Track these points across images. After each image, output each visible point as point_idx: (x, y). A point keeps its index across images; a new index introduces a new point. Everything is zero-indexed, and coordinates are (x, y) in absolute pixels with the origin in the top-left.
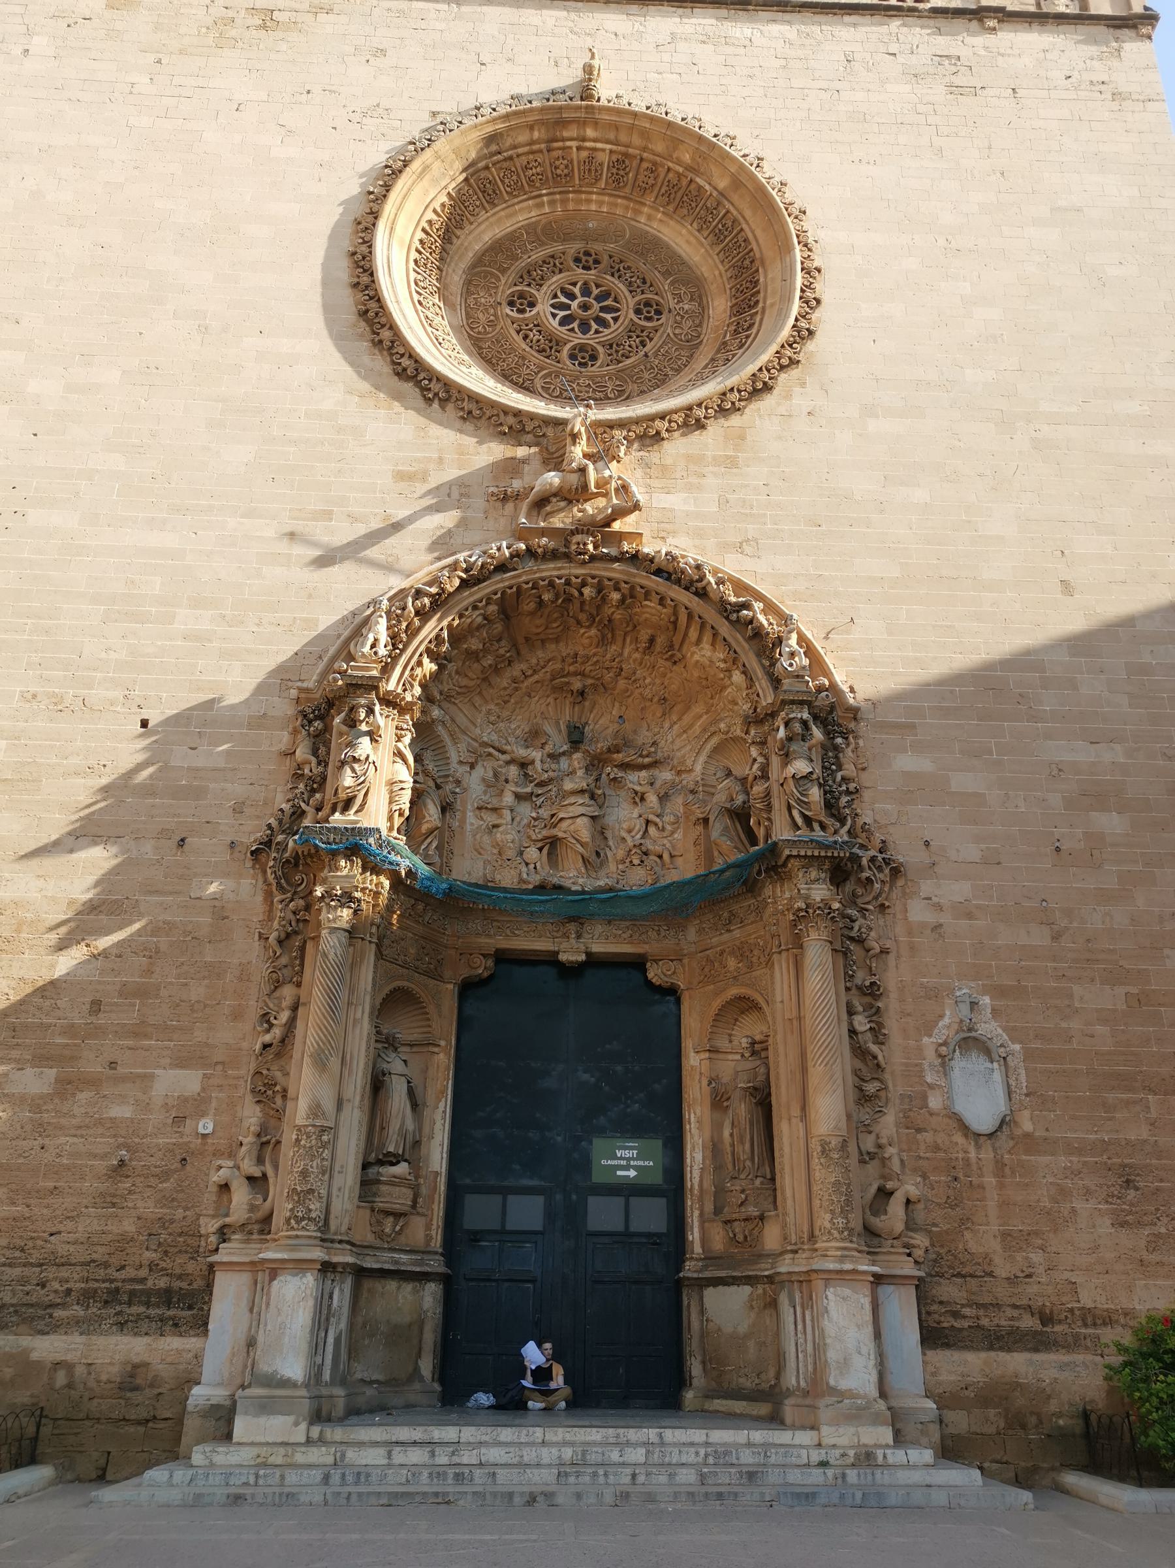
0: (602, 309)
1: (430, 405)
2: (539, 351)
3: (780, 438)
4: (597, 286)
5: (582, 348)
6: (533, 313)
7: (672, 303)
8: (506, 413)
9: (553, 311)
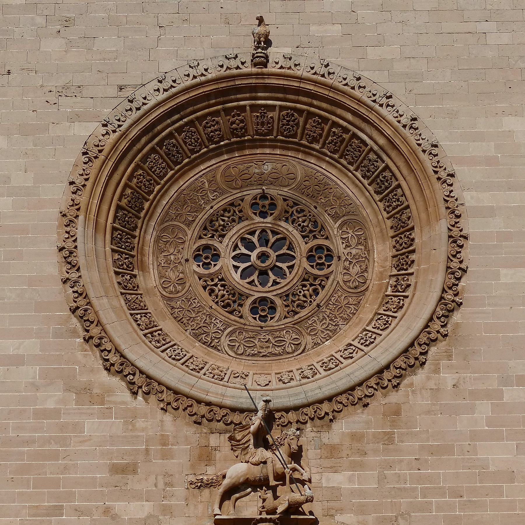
0: (280, 258)
1: (136, 398)
2: (224, 307)
3: (429, 412)
4: (274, 233)
5: (263, 300)
6: (217, 268)
7: (341, 247)
8: (199, 402)
9: (236, 264)
